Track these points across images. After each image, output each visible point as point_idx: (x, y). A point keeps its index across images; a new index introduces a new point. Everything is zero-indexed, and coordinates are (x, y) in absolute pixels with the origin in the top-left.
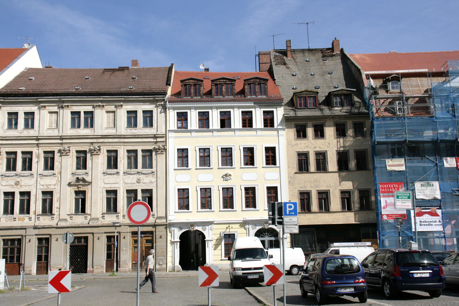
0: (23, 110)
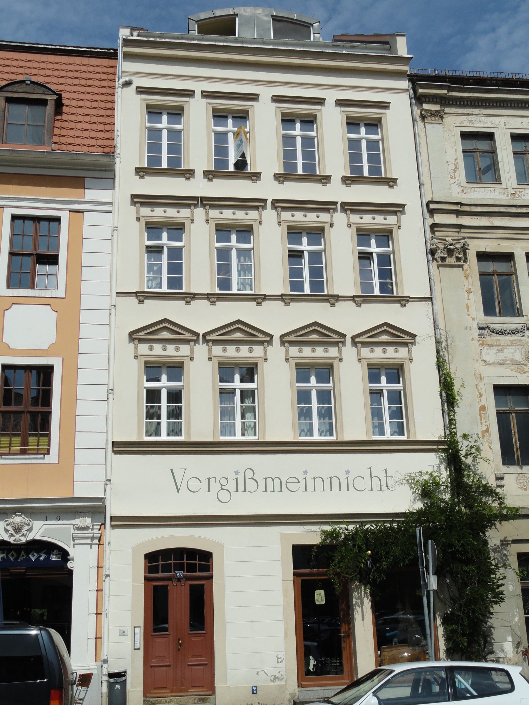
0: (507, 126)
